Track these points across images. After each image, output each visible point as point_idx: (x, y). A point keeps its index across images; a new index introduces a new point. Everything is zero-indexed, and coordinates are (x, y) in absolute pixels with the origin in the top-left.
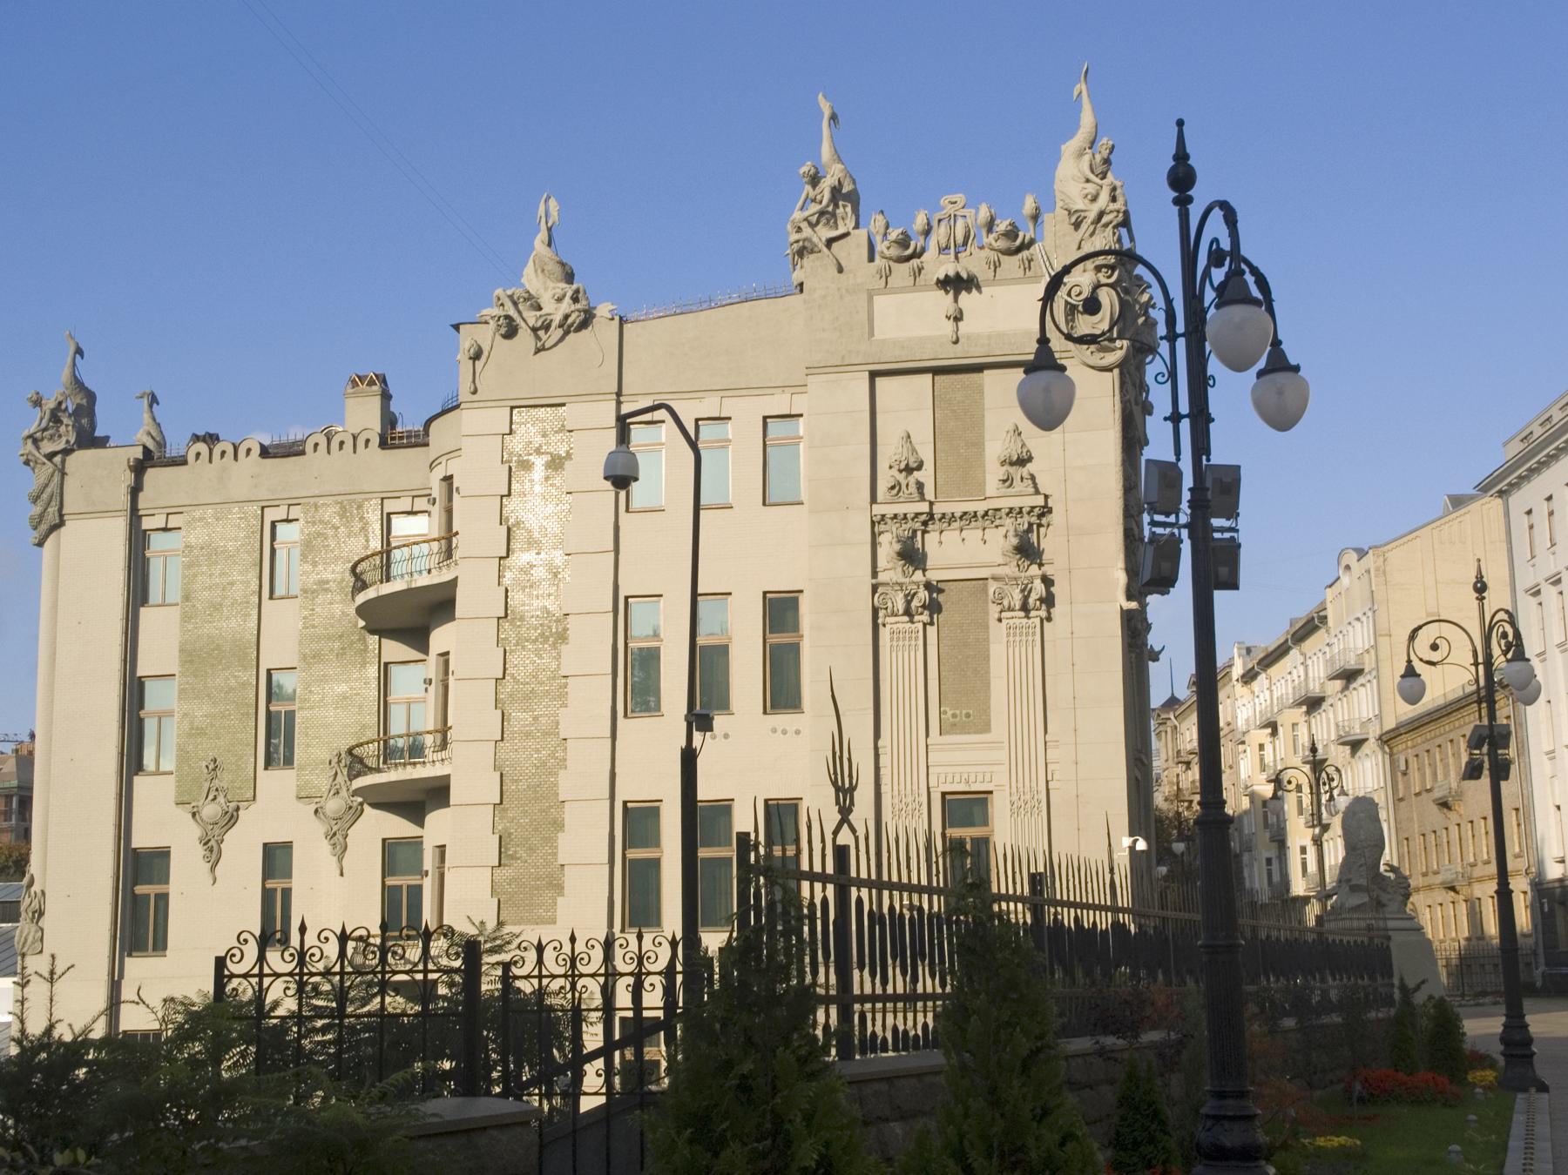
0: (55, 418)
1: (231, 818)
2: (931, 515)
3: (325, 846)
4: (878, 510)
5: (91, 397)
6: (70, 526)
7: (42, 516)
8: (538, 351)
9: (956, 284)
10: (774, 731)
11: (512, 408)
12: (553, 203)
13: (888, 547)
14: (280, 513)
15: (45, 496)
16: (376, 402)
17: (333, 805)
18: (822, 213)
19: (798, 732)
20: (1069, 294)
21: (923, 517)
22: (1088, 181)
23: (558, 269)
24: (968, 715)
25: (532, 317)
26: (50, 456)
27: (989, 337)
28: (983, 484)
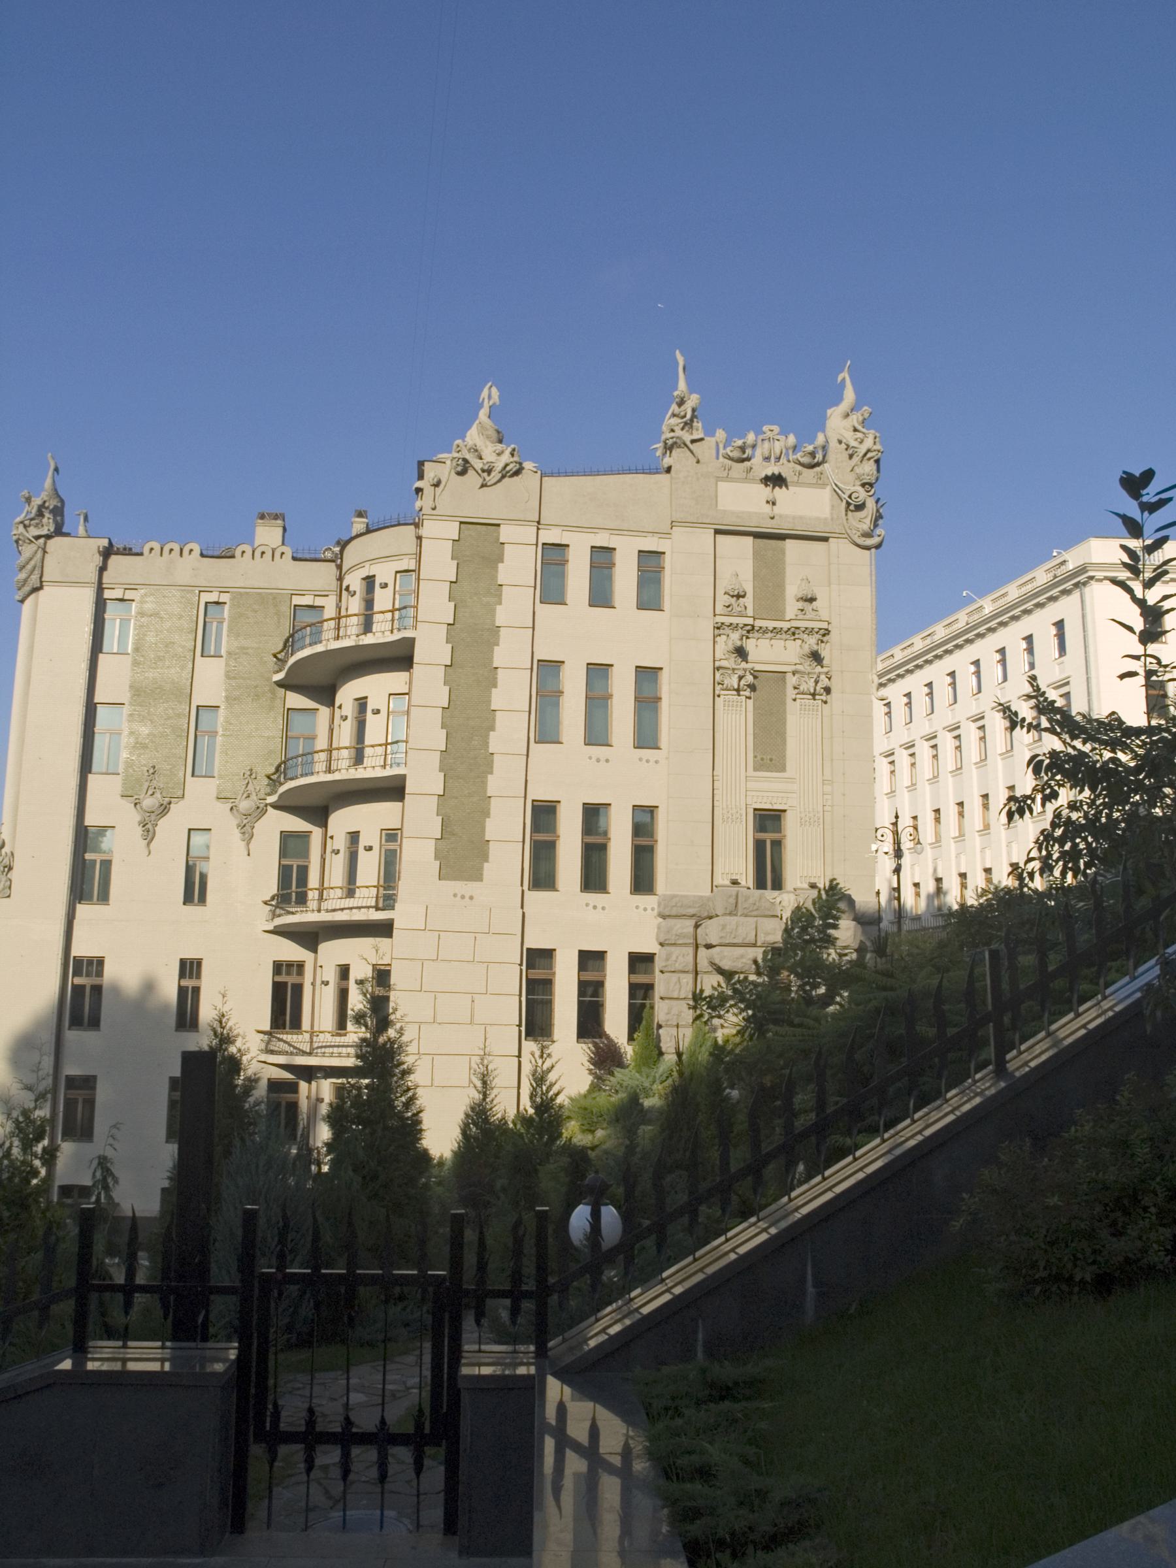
0: (40, 514)
1: (164, 809)
2: (753, 626)
3: (237, 833)
4: (720, 619)
5: (62, 501)
6: (47, 590)
7: (25, 581)
8: (483, 486)
9: (777, 481)
10: (640, 760)
11: (461, 523)
12: (494, 391)
13: (725, 644)
14: (213, 597)
15: (29, 567)
16: (280, 530)
17: (245, 805)
18: (686, 424)
19: (657, 762)
20: (850, 497)
21: (749, 628)
22: (855, 430)
23: (495, 436)
24: (771, 760)
25: (478, 465)
26: (38, 537)
27: (794, 518)
28: (783, 612)
